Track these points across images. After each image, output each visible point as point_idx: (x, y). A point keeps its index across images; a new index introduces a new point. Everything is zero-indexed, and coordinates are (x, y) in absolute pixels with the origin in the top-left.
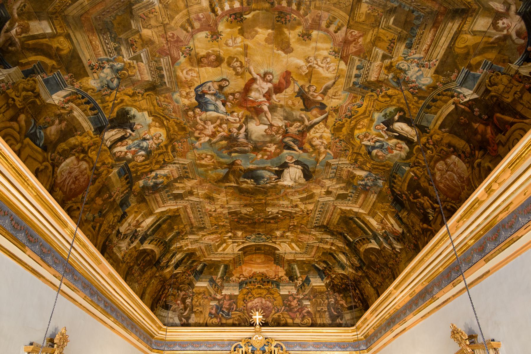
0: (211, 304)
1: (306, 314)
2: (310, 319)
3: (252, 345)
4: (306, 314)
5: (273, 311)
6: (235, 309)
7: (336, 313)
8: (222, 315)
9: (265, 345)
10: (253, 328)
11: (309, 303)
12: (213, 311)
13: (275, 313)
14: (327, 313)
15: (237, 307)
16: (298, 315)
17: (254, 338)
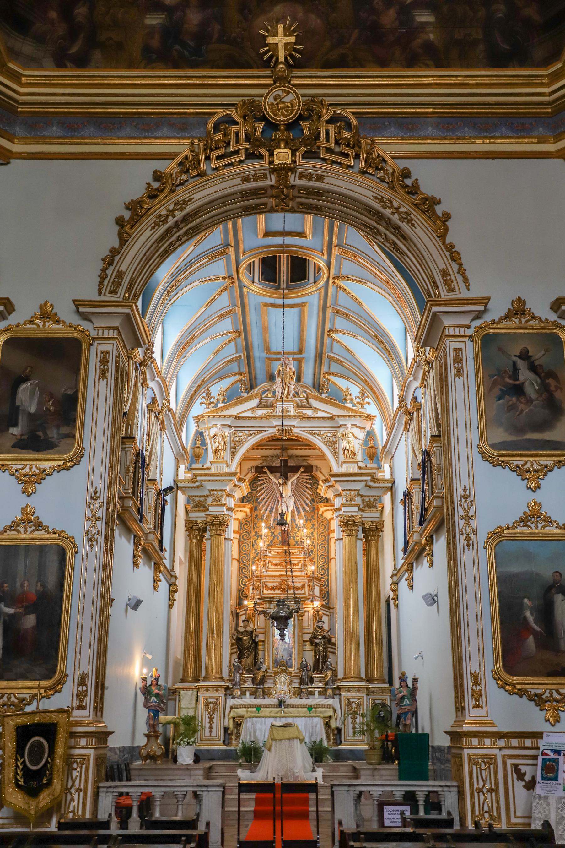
3: (263, 118)
10: (268, 73)
17: (271, 100)
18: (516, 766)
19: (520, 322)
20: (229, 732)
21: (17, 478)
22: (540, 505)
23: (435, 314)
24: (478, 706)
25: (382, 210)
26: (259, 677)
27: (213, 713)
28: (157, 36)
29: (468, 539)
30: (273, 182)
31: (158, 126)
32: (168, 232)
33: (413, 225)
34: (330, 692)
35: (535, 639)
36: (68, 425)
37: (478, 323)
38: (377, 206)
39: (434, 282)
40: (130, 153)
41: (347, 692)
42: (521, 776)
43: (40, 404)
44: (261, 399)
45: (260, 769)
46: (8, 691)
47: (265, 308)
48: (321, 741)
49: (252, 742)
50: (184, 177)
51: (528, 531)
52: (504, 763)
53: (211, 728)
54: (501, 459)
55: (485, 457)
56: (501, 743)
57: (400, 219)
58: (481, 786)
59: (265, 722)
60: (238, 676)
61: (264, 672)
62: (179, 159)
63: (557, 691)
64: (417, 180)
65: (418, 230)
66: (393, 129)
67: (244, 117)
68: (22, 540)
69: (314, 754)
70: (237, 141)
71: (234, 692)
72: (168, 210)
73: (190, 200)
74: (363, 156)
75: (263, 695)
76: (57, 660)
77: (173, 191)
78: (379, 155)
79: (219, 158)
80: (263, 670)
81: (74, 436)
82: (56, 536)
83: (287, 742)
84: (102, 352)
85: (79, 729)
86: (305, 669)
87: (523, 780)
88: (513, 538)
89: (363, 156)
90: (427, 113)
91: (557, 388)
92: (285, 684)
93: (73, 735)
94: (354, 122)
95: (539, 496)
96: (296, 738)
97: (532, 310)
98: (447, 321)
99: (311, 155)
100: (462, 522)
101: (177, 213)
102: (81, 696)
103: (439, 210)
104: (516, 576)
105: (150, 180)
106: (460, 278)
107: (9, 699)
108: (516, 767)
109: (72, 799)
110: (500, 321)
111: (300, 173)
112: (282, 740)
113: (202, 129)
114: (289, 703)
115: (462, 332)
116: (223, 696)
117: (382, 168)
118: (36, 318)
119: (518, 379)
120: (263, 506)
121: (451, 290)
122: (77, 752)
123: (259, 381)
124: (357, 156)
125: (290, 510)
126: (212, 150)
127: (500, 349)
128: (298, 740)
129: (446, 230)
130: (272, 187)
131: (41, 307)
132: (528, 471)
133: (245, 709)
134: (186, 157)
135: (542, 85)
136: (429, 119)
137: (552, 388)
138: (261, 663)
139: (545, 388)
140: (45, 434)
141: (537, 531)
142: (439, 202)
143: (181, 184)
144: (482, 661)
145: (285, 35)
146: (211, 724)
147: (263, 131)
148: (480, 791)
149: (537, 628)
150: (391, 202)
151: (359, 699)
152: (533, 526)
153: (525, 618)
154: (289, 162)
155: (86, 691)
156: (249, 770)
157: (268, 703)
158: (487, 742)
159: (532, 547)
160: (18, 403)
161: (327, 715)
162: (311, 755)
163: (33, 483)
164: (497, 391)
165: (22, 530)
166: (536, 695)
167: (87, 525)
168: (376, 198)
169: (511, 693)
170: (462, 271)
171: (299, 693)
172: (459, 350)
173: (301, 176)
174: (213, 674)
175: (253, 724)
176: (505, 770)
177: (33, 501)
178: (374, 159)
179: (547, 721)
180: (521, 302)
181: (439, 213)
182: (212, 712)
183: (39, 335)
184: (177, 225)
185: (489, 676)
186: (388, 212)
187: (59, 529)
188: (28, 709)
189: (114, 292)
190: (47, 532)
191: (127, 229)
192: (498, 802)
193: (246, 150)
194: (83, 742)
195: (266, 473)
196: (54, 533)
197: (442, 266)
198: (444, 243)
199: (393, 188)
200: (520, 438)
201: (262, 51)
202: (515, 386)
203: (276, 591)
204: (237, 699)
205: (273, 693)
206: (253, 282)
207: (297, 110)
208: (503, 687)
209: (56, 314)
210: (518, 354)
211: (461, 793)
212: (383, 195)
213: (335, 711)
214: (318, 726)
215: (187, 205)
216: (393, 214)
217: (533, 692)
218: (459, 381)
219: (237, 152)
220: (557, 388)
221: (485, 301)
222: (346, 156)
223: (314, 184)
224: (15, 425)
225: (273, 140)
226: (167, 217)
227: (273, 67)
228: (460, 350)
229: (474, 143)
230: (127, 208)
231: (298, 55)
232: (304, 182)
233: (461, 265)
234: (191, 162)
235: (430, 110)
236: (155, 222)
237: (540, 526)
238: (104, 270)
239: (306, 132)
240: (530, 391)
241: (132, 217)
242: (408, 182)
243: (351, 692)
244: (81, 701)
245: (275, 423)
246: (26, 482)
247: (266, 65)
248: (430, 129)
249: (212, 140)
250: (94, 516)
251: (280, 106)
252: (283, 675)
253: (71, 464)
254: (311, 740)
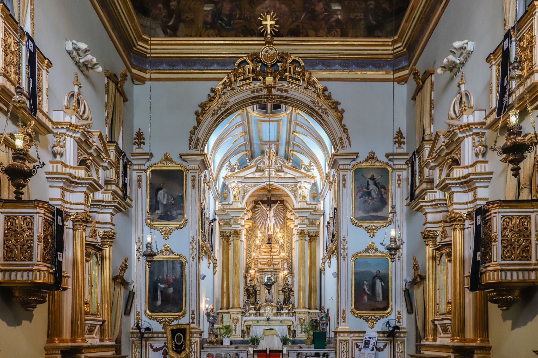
0: (205, 9)
1: (334, 24)
2: (339, 30)
3: (260, 62)
4: (334, 24)
5: (291, 20)
6: (238, 16)
7: (374, 23)
8: (221, 25)
9: (278, 61)
11: (339, 8)
12: (209, 19)
13: (293, 22)
14: (362, 22)
15: (240, 14)
16: (323, 26)
18: (356, 344)
19: (372, 162)
21: (161, 232)
22: (374, 243)
23: (335, 160)
24: (344, 322)
25: (314, 107)
28: (210, 16)
29: (344, 257)
30: (265, 94)
31: (212, 64)
32: (218, 117)
33: (328, 115)
35: (367, 297)
36: (180, 209)
37: (354, 163)
38: (312, 105)
39: (336, 143)
40: (200, 78)
42: (358, 346)
43: (168, 200)
44: (258, 166)
46: (165, 317)
47: (260, 122)
50: (225, 90)
51: (368, 254)
52: (352, 342)
54: (359, 224)
55: (353, 223)
56: (352, 335)
57: (322, 112)
58: (343, 350)
62: (223, 81)
63: (374, 316)
64: (330, 93)
65: (330, 118)
66: (320, 66)
67: (252, 61)
68: (165, 258)
70: (249, 73)
72: (218, 107)
73: (228, 102)
74: (306, 79)
76: (183, 305)
77: (220, 98)
78: (313, 80)
79: (240, 81)
81: (183, 214)
82: (179, 256)
84: (192, 176)
85: (193, 331)
87: (358, 348)
88: (362, 257)
89: (306, 79)
90: (336, 58)
91: (385, 193)
93: (192, 333)
94: (302, 63)
95: (374, 240)
97: (377, 157)
98: (340, 162)
99: (283, 79)
100: (342, 251)
101: (222, 109)
102: (193, 318)
103: (340, 107)
104: (362, 272)
105: (209, 92)
106: (347, 141)
107: (165, 319)
108: (356, 344)
109: (192, 355)
110: (363, 163)
111: (278, 89)
113: (232, 65)
115: (347, 168)
117: (315, 87)
118: (163, 161)
119: (368, 189)
120: (259, 221)
121: (342, 147)
122: (193, 339)
123: (256, 154)
124: (304, 80)
125: (272, 224)
126: (237, 77)
127: (363, 176)
129: (342, 118)
130: (265, 95)
131: (165, 155)
132: (370, 229)
134: (226, 81)
135: (388, 45)
136: (337, 61)
137: (383, 193)
139: (380, 193)
140: (170, 212)
141: (372, 254)
142: (340, 104)
143: (224, 94)
144: (346, 305)
145: (271, 20)
147: (261, 66)
148: (342, 352)
149: (369, 293)
150: (318, 103)
152: (370, 252)
153: (364, 289)
154: (273, 84)
155: (195, 317)
158: (346, 335)
159: (369, 261)
160: (158, 200)
163: (167, 234)
164: (360, 194)
165: (165, 254)
166: (366, 318)
167: (191, 252)
168: (312, 101)
169: (357, 317)
170: (348, 138)
171: (277, 314)
172: (344, 175)
173: (278, 90)
176: (352, 344)
177: (168, 242)
178: (311, 82)
179: (369, 327)
180: (373, 153)
181: (340, 109)
183: (165, 169)
184: (222, 114)
185: (349, 311)
186: (316, 109)
187: (179, 253)
188: (173, 323)
189: (196, 148)
190: (175, 255)
191: (200, 117)
192: (348, 355)
193: (253, 77)
194: (195, 335)
195: (260, 204)
196: (178, 255)
197: (340, 135)
198: (341, 124)
199: (319, 96)
200: (368, 215)
201: (260, 28)
202: (368, 192)
203: (266, 266)
206: (254, 111)
207: (277, 57)
208: (354, 315)
209: (171, 159)
210: (370, 177)
211: (336, 353)
212: (314, 100)
215: (226, 105)
216: (319, 110)
217: (365, 316)
218: (344, 190)
219: (248, 78)
220: (385, 193)
221: (357, 155)
222: (298, 80)
223: (284, 94)
224: (158, 209)
225: (265, 73)
226: (218, 111)
227: (265, 36)
228: (345, 175)
229: (356, 74)
230: (200, 106)
231: (277, 30)
232: (279, 93)
233: (348, 135)
234: (227, 83)
235: (338, 56)
236: (212, 114)
237: (373, 252)
238: (191, 137)
239: (280, 68)
240: (374, 194)
241: (202, 111)
242: (326, 93)
244: (193, 320)
245: (265, 181)
246: (164, 234)
247: (261, 35)
248: (337, 66)
249: (237, 72)
250: (193, 248)
251: (269, 56)
253: (182, 226)
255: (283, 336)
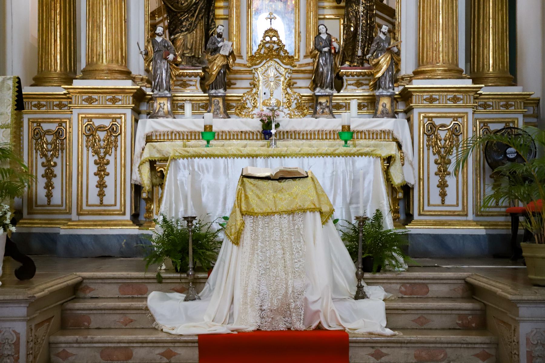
20: (144, 195)
26: (215, 69)
27: (106, 153)
34: (385, 103)
41: (426, 103)
45: (211, 291)
48: (378, 216)
49: (189, 220)
53: (101, 185)
59: (226, 168)
60: (163, 66)
61: (227, 57)
69: (360, 251)
71: (156, 105)
75: (225, 112)
80: (225, 52)
83: (286, 220)
86: (326, 49)
92: (277, 84)
96: (312, 210)
112: (273, 213)
114: (288, 128)
116: (129, 112)
128: (318, 215)
133: (179, 143)
138: (220, 36)
146: (101, 178)
151: (455, 118)
156: (180, 291)
157: (236, 129)
161: (385, 153)
162: (353, 254)
174: (104, 63)
175: (193, 173)
182: (102, 151)
204: (161, 120)
205: (249, 105)
213: (400, 146)
214: (370, 177)
243: (436, 103)
252: (271, 63)
254: (348, 213)
255: (362, 220)
